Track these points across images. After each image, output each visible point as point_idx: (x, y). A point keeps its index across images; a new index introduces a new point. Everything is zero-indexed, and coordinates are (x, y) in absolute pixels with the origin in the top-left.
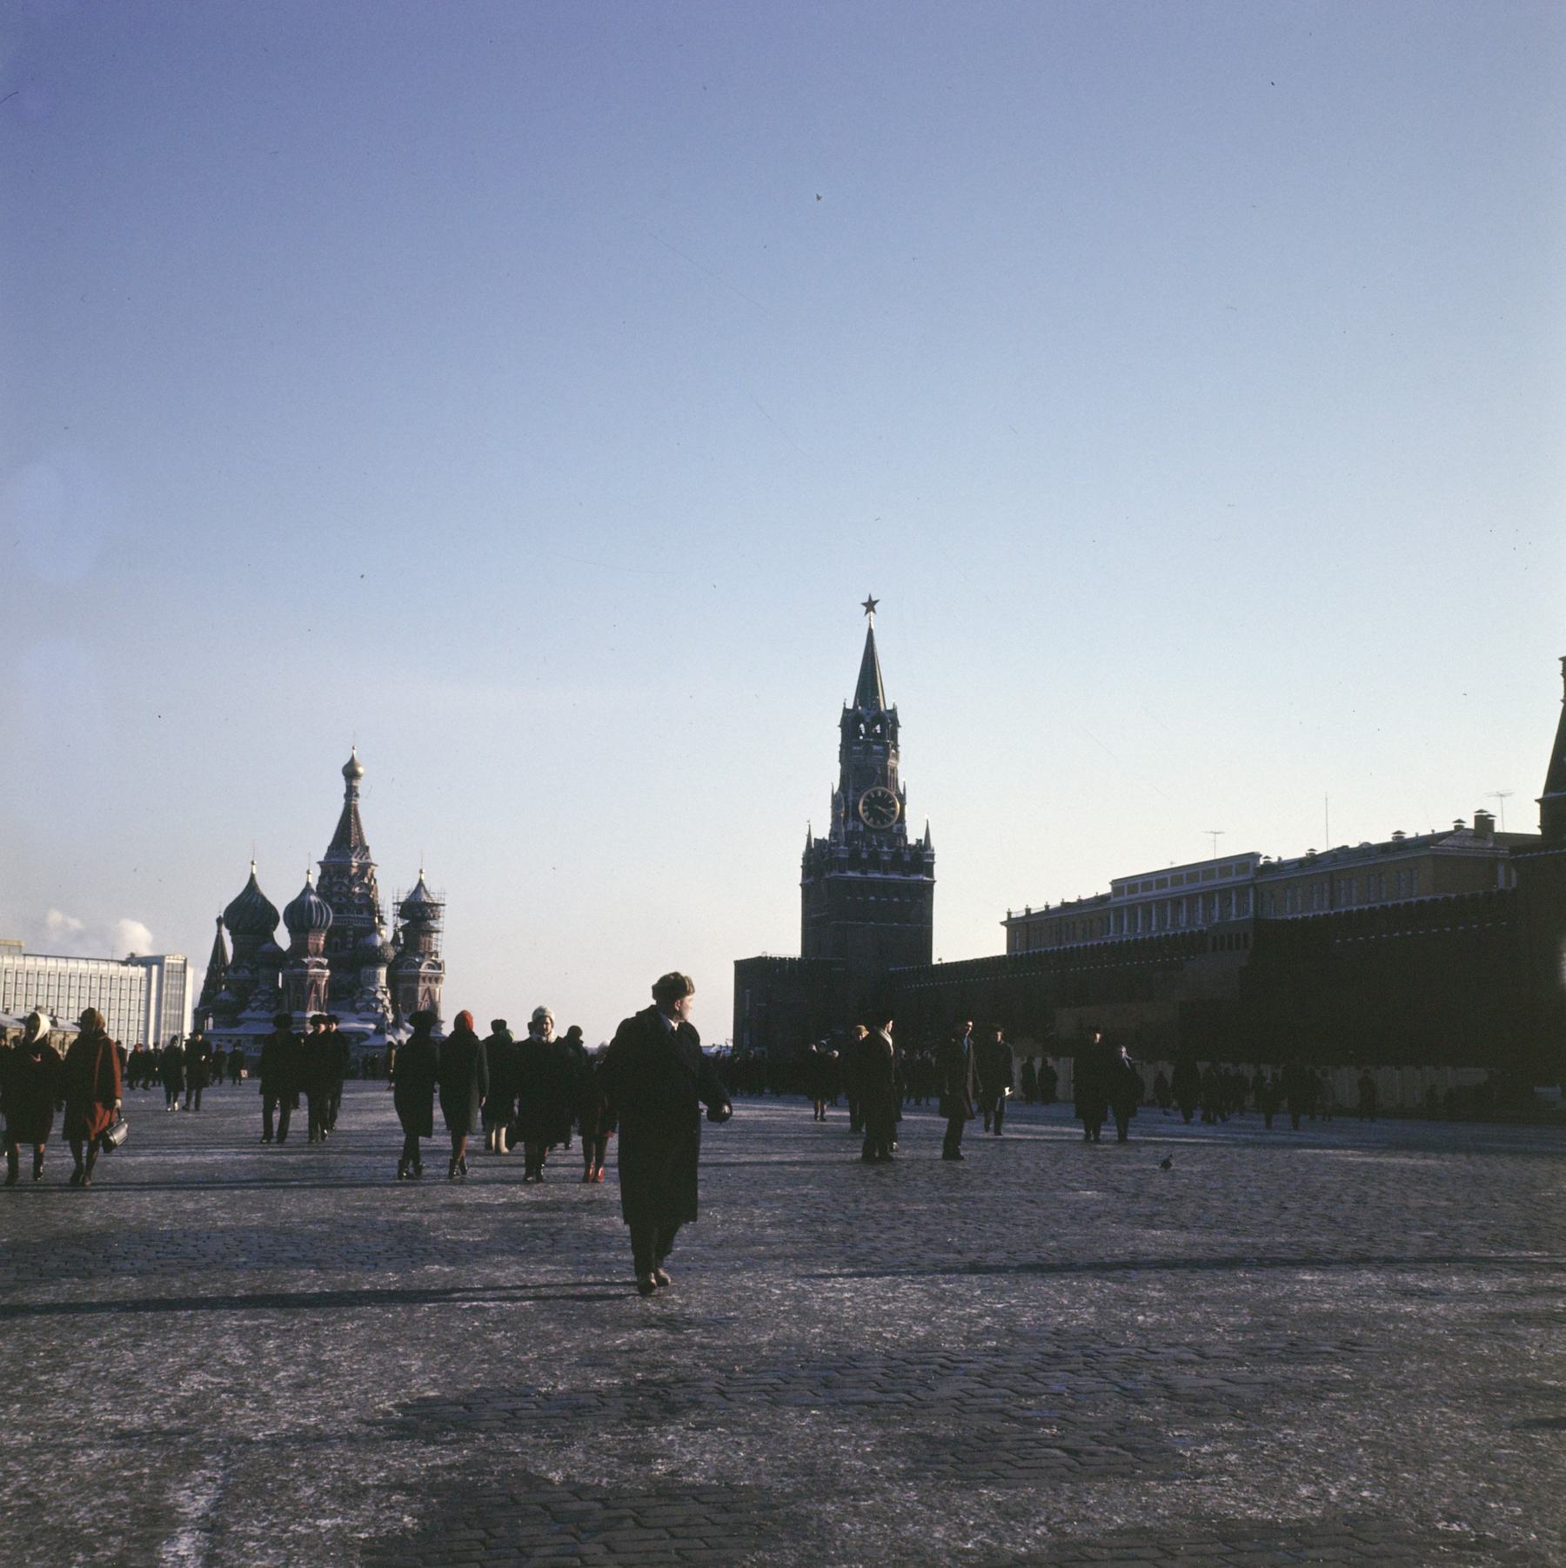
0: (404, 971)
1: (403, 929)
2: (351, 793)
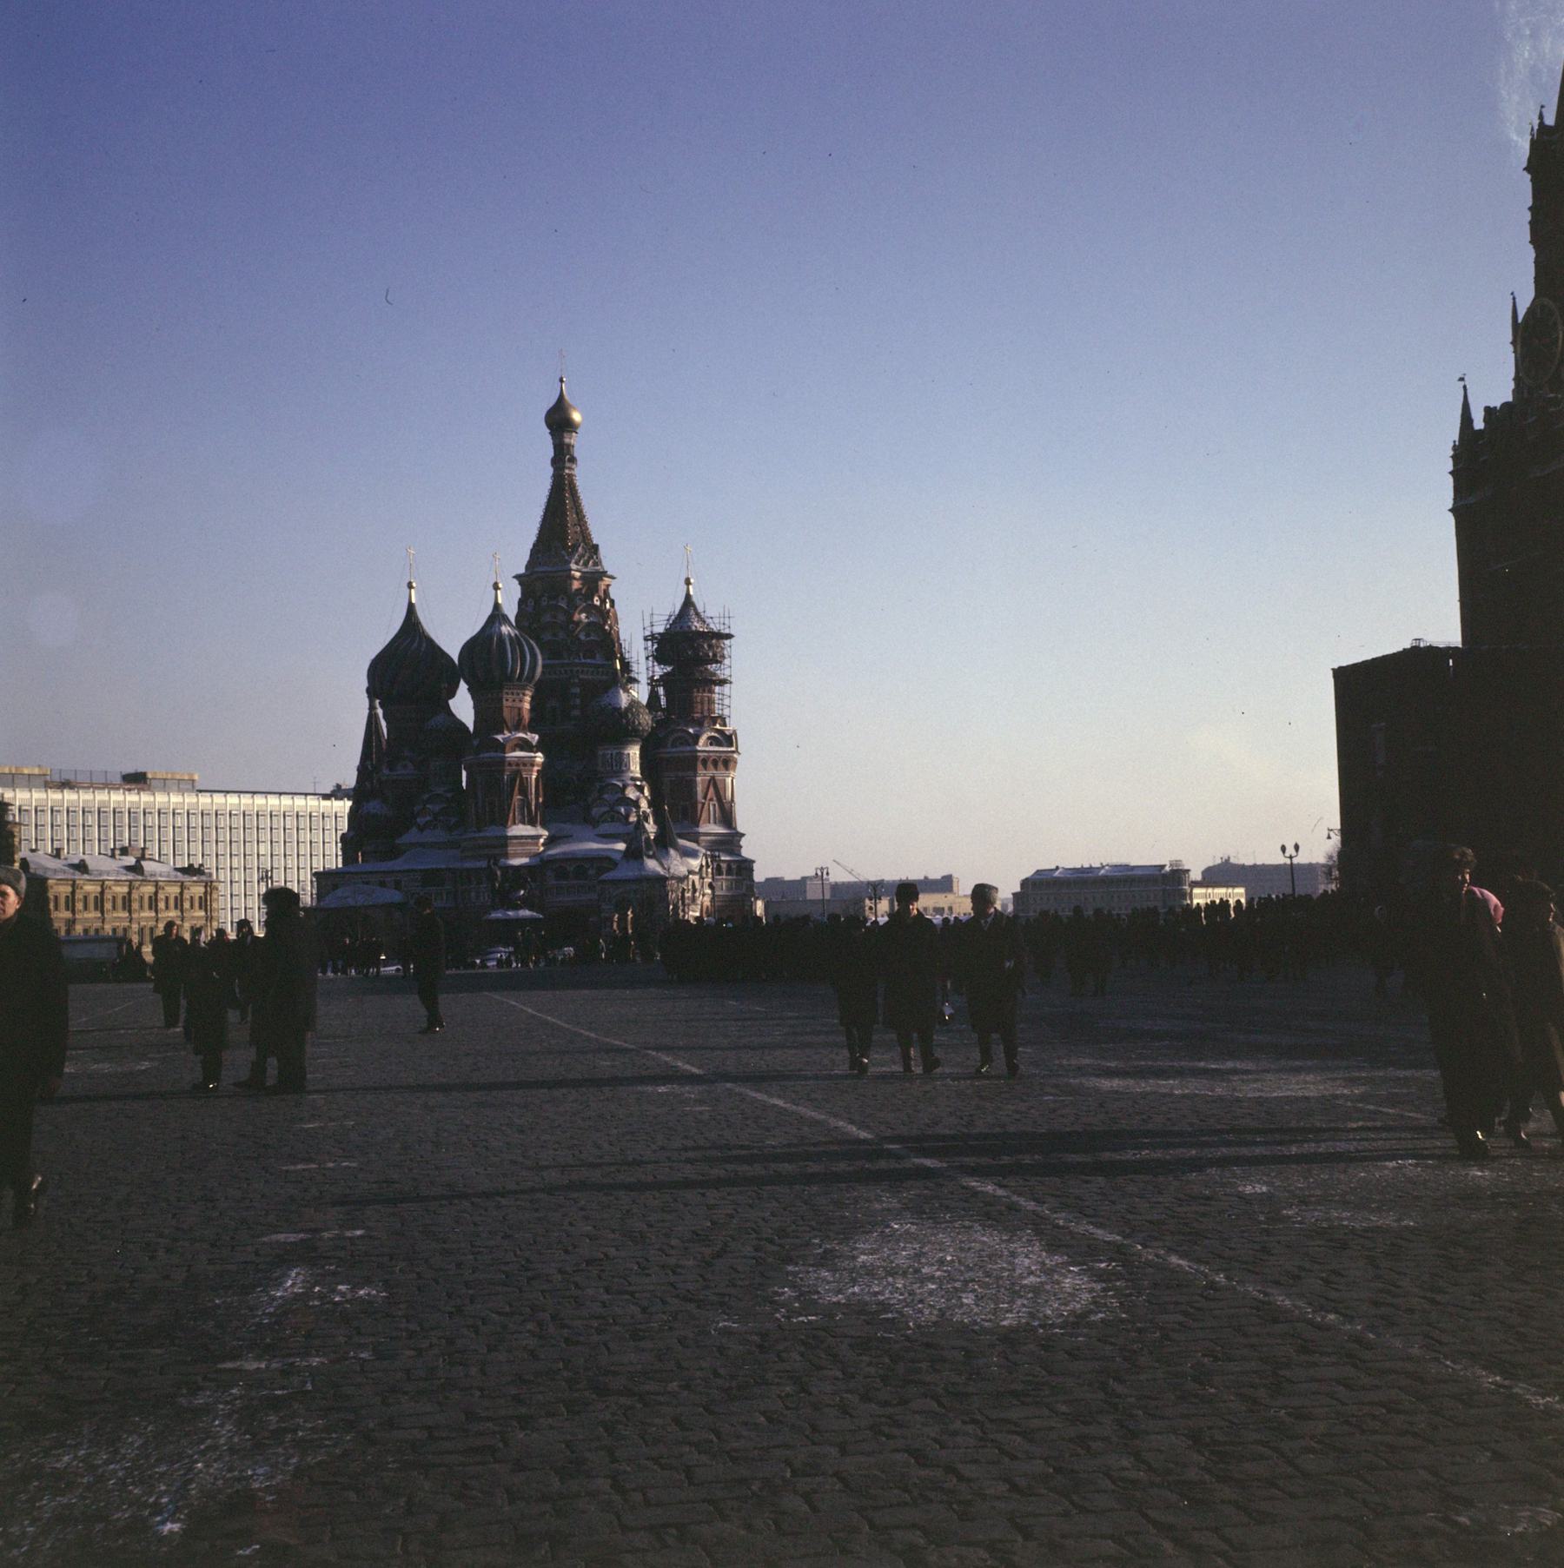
0: (670, 751)
1: (664, 679)
2: (562, 457)
